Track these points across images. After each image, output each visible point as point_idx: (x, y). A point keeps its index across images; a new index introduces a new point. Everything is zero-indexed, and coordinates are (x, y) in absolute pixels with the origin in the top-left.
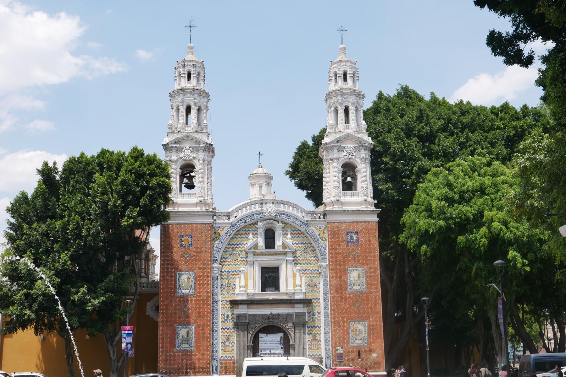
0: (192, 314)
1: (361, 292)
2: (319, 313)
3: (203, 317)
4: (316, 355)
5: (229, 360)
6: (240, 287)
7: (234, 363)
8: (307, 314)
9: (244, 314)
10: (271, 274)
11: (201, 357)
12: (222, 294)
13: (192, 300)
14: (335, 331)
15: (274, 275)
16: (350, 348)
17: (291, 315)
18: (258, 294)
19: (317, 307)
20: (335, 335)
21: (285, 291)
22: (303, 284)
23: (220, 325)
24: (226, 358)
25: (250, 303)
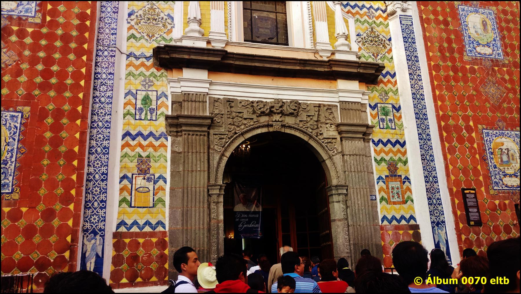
0: (19, 72)
1: (495, 62)
2: (398, 109)
3: (61, 88)
4: (403, 217)
5: (145, 235)
6: (188, 22)
7: (162, 244)
9: (197, 94)
10: (265, 14)
11: (39, 223)
12: (133, 36)
13: (22, 34)
14: (452, 150)
15: (272, 16)
16: (494, 197)
17: (330, 108)
18: (239, 44)
19: (390, 94)
20: (454, 162)
21: (309, 46)
22: (353, 37)
23: (119, 127)
24: (135, 229)
25: (219, 62)
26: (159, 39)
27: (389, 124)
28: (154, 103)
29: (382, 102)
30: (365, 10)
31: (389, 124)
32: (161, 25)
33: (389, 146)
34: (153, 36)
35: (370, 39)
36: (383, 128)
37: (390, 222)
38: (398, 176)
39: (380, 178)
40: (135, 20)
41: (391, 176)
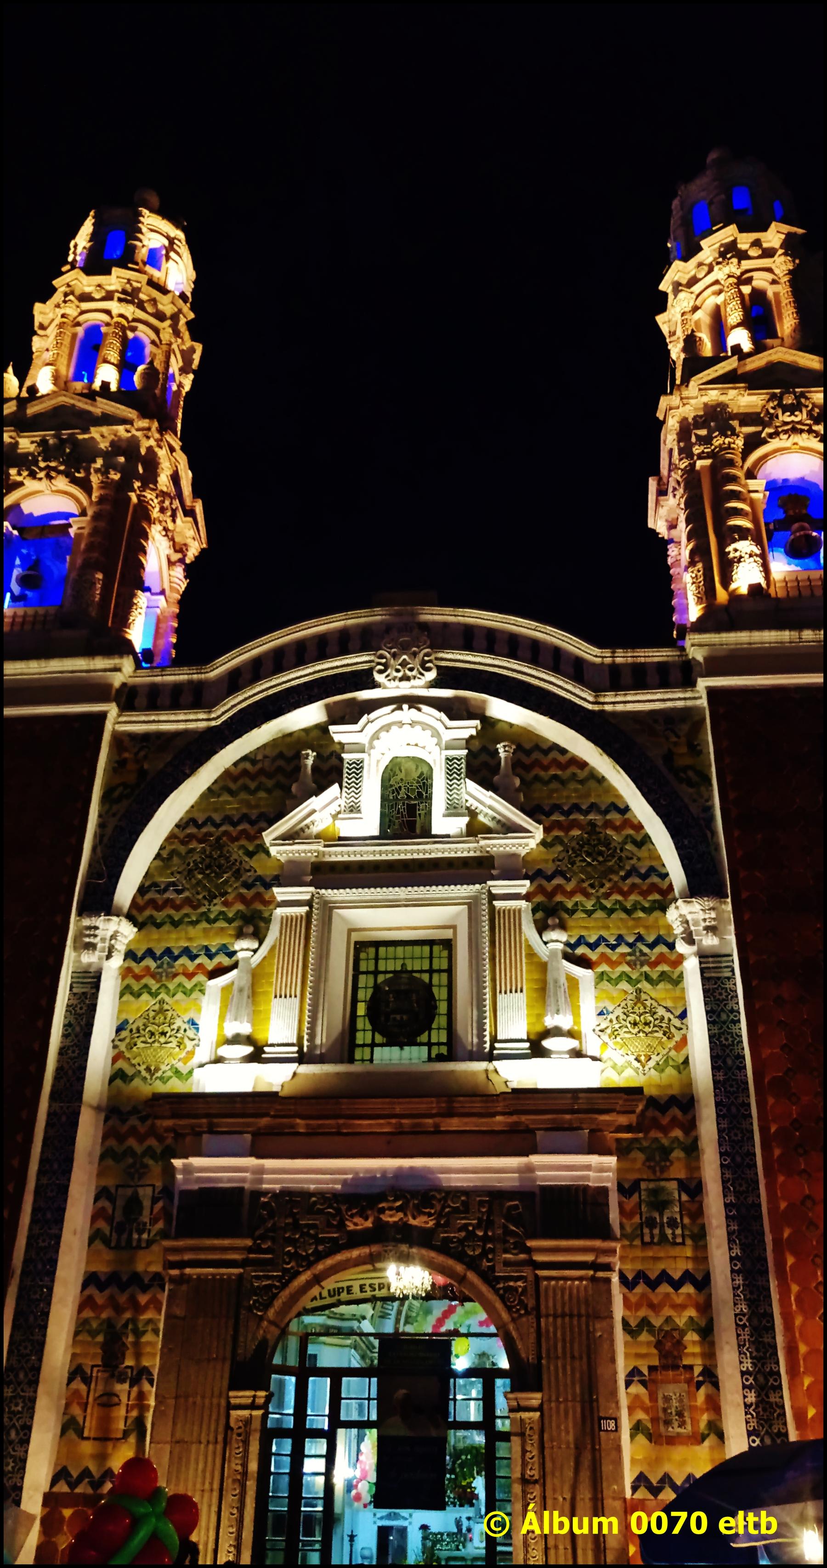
8: (614, 1199)
26: (169, 1074)
27: (669, 1231)
28: (146, 1212)
29: (652, 1177)
30: (624, 949)
31: (669, 1231)
32: (174, 1044)
33: (665, 1288)
34: (157, 1069)
35: (632, 1018)
36: (652, 1243)
37: (655, 1491)
38: (685, 1367)
39: (633, 1375)
40: (127, 1040)
41: (665, 1367)
